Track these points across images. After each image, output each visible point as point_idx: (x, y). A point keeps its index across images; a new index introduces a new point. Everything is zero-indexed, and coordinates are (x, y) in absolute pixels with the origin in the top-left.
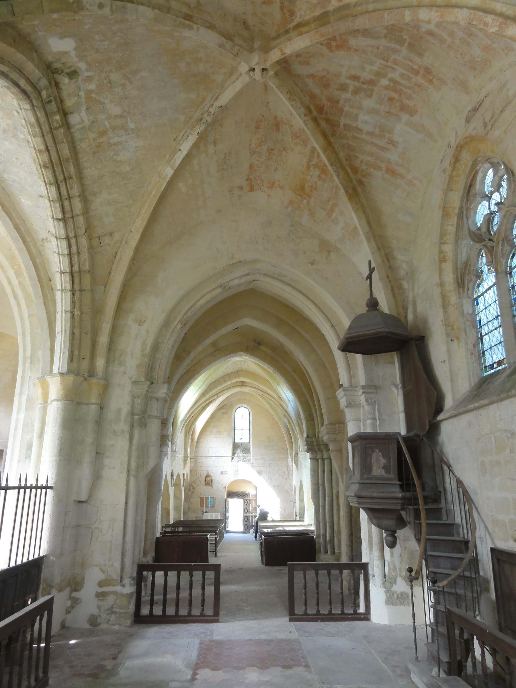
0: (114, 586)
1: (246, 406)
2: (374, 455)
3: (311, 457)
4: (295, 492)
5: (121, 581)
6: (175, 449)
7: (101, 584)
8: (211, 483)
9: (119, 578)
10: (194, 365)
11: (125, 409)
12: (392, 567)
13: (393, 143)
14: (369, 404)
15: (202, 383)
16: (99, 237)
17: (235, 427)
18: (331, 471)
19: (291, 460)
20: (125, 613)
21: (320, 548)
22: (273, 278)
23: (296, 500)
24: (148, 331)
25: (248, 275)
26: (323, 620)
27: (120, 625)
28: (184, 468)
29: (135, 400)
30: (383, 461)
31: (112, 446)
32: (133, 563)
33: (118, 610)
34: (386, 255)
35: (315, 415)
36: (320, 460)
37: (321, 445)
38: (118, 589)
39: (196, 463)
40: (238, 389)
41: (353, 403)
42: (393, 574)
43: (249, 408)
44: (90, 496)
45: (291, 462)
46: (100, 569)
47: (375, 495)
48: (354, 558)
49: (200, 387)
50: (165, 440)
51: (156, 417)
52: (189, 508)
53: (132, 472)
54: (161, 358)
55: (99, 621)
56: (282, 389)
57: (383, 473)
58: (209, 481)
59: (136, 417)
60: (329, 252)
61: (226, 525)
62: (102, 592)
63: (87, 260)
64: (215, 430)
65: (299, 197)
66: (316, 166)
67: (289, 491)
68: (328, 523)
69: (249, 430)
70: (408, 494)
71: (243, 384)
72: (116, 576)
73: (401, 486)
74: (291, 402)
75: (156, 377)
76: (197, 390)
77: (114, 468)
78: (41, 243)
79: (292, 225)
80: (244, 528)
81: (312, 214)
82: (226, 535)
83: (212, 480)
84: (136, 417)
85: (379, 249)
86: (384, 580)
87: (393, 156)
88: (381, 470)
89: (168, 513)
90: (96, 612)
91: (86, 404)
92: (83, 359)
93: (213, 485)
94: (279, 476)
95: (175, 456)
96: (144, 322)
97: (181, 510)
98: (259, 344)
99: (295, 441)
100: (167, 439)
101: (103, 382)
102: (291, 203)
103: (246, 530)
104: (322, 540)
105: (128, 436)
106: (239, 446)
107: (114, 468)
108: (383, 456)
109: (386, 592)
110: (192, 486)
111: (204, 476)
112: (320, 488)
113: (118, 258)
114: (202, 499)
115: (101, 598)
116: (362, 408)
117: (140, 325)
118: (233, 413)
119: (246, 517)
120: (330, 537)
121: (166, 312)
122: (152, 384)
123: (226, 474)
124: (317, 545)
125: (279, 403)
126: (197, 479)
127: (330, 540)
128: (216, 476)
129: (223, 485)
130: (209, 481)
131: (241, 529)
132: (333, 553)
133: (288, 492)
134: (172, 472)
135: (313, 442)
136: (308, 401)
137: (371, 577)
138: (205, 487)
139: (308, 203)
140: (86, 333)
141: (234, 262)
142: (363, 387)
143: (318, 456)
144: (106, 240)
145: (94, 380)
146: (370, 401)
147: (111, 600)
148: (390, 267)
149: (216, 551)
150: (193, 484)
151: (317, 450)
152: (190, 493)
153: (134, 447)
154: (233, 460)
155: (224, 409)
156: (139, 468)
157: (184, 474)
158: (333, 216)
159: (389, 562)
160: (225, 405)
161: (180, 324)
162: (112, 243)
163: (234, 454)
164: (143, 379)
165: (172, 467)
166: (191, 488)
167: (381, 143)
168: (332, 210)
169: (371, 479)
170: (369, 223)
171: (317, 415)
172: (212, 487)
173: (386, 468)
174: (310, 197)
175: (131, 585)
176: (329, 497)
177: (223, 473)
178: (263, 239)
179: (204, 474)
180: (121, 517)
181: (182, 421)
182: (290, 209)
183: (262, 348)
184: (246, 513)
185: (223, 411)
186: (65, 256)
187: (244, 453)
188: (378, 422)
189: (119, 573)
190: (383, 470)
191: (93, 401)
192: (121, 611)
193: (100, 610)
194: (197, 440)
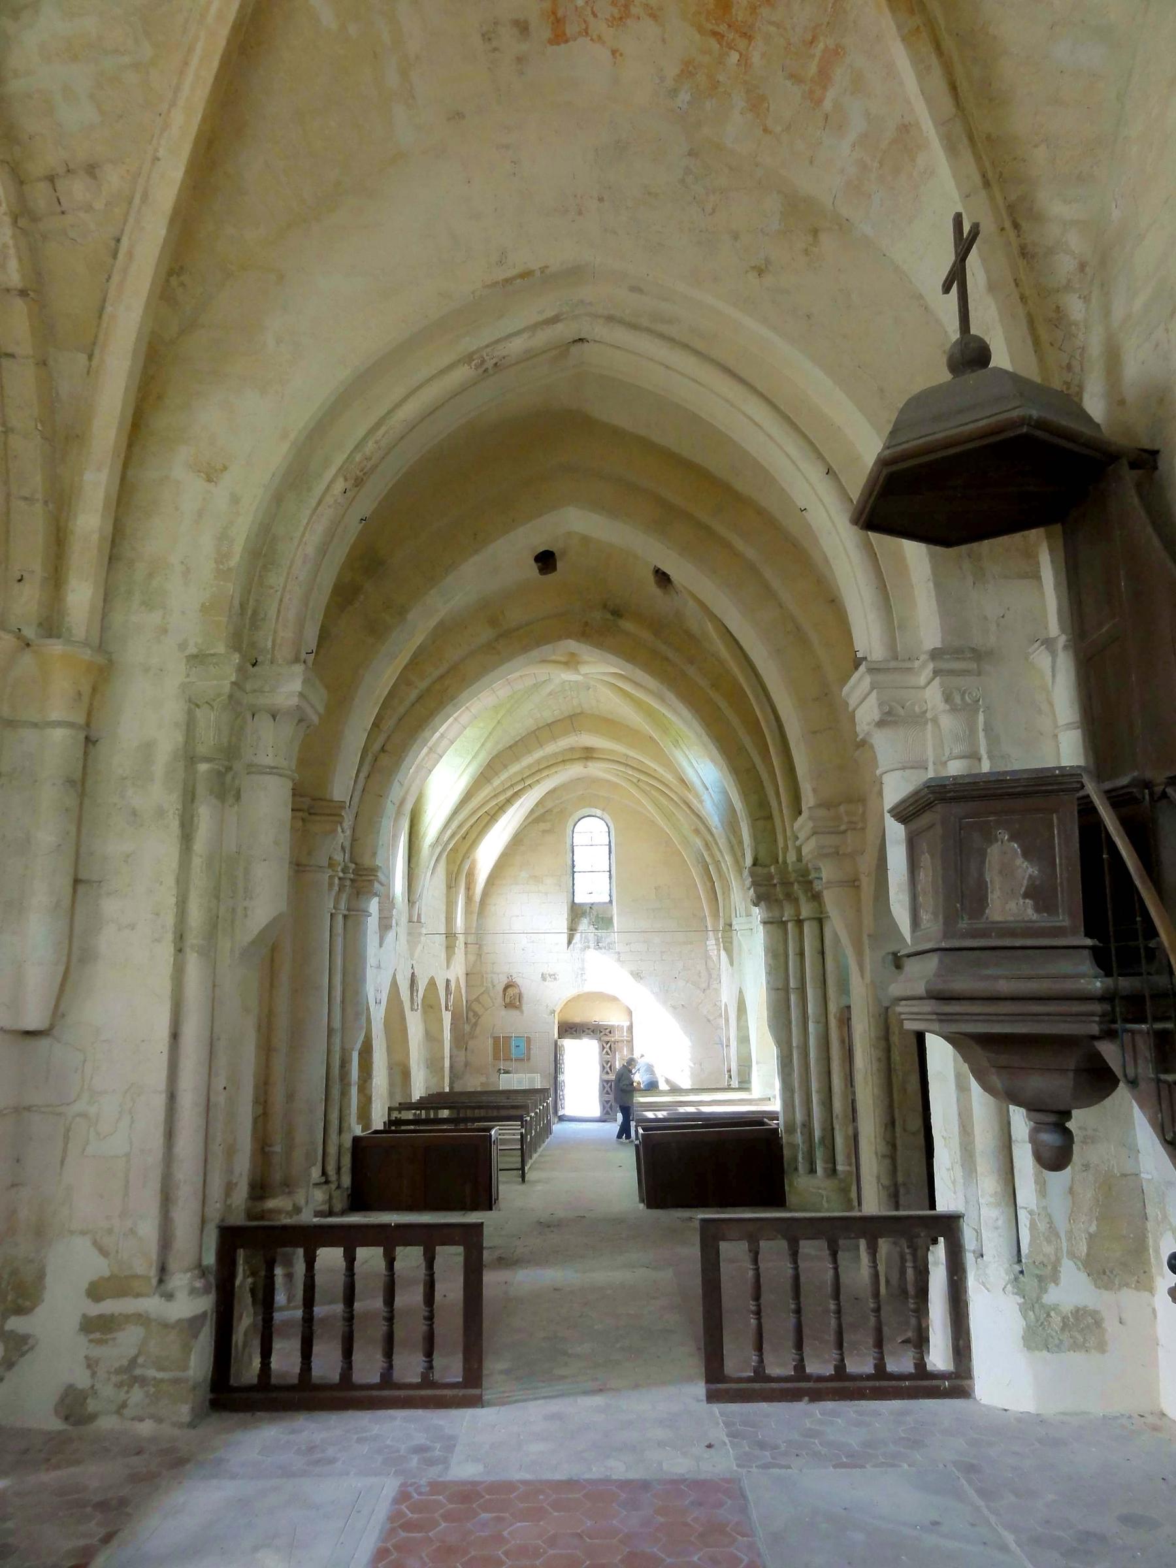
0: (138, 1295)
1: (599, 812)
2: (994, 853)
3: (766, 916)
4: (727, 1020)
5: (161, 1281)
6: (419, 915)
7: (95, 1292)
9: (153, 1273)
10: (442, 677)
11: (168, 743)
12: (1042, 1226)
14: (954, 709)
15: (479, 745)
16: (51, 179)
17: (573, 866)
18: (822, 953)
20: (176, 1381)
21: (795, 1159)
22: (634, 327)
23: (728, 1039)
24: (235, 500)
25: (555, 320)
26: (816, 1396)
27: (159, 1420)
28: (448, 967)
29: (198, 713)
30: (1026, 870)
31: (127, 857)
32: (203, 1222)
33: (152, 1373)
34: (1011, 208)
35: (774, 803)
36: (790, 925)
37: (792, 884)
38: (152, 1305)
39: (479, 955)
40: (575, 770)
41: (902, 712)
42: (1049, 1249)
43: (606, 817)
44: (58, 1013)
45: (715, 947)
46: (95, 1243)
47: (1004, 987)
48: (902, 1191)
49: (474, 757)
50: (369, 881)
51: (273, 770)
52: (467, 1064)
53: (194, 939)
54: (282, 585)
55: (92, 1406)
56: (687, 756)
57: (1030, 911)
58: (512, 997)
59: (203, 767)
60: (815, 232)
61: (559, 1103)
62: (100, 1316)
63: (12, 251)
64: (524, 875)
65: (713, 44)
67: (711, 1018)
68: (817, 1092)
69: (610, 871)
70: (1125, 984)
71: (588, 755)
72: (144, 1266)
73: (1101, 959)
74: (710, 790)
75: (269, 644)
76: (468, 764)
77: (132, 927)
79: (692, 153)
81: (757, 104)
82: (557, 1128)
83: (520, 995)
84: (203, 767)
85: (987, 184)
86: (1017, 1268)
88: (1021, 901)
89: (406, 1075)
90: (82, 1379)
91: (35, 725)
92: (20, 581)
93: (525, 1007)
95: (420, 934)
96: (222, 471)
97: (443, 1068)
98: (617, 613)
99: (724, 893)
100: (372, 878)
101: (87, 655)
102: (688, 70)
103: (607, 1113)
104: (799, 1138)
105: (175, 825)
107: (133, 929)
108: (1026, 854)
109: (1024, 1310)
111: (500, 988)
112: (793, 998)
113: (121, 256)
114: (496, 1040)
115: (98, 1335)
116: (929, 726)
117: (209, 480)
118: (569, 831)
120: (823, 1130)
121: (292, 436)
122: (254, 665)
123: (555, 979)
124: (786, 1152)
125: (681, 798)
126: (482, 993)
127: (823, 1139)
128: (529, 984)
129: (547, 1006)
130: (514, 999)
131: (596, 1112)
132: (833, 1172)
133: (709, 1021)
134: (413, 973)
135: (771, 877)
136: (754, 767)
137: (969, 1259)
138: (504, 1012)
139: (745, 61)
140: (26, 499)
141: (510, 273)
142: (935, 654)
143: (786, 914)
144: (77, 189)
145: (56, 648)
146: (958, 700)
147: (128, 1340)
148: (1024, 252)
149: (523, 1169)
150: (477, 1007)
151: (781, 897)
152: (467, 1028)
153: (197, 862)
154: (572, 945)
155: (544, 822)
156: (213, 926)
157: (448, 981)
158: (828, 105)
159: (1031, 1213)
161: (341, 479)
162: (99, 205)
163: (572, 930)
164: (221, 648)
165: (414, 962)
166: (471, 1014)
168: (824, 77)
169: (984, 934)
170: (953, 88)
171: (780, 803)
172: (522, 1012)
173: (1039, 894)
174: (748, 36)
175: (193, 1291)
176: (818, 1023)
177: (548, 979)
178: (601, 200)
179: (504, 981)
180: (157, 1077)
181: (433, 846)
182: (684, 97)
183: (628, 625)
184: (607, 1073)
185: (543, 826)
189: (154, 1256)
190: (1027, 901)
191: (54, 716)
192: (160, 1375)
193: (94, 1374)
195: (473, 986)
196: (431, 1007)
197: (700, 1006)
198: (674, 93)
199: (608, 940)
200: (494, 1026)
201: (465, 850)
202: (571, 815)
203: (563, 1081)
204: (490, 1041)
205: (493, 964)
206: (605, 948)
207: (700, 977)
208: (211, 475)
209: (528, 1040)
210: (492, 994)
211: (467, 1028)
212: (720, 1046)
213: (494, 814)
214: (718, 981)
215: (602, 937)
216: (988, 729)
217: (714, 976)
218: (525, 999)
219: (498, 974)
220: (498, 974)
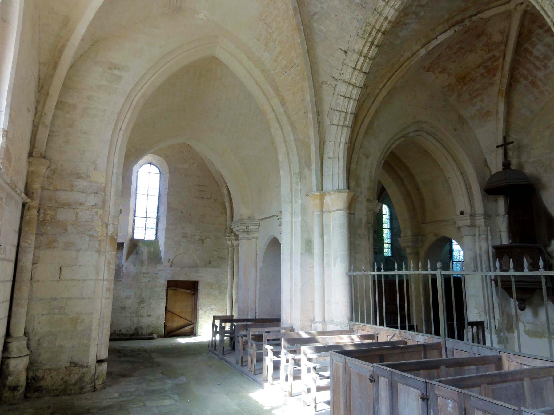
13: (546, 66)
22: (430, 135)
24: (372, 164)
25: (417, 131)
65: (457, 83)
66: (486, 67)
78: (320, 84)
81: (459, 96)
86: (496, 330)
87: (540, 74)
102: (449, 85)
105: (367, 238)
109: (498, 337)
158: (474, 101)
159: (498, 320)
167: (538, 64)
168: (475, 97)
182: (446, 89)
186: (356, 101)
188: (489, 237)
198: (444, 88)
208: (367, 157)
216: (490, 230)
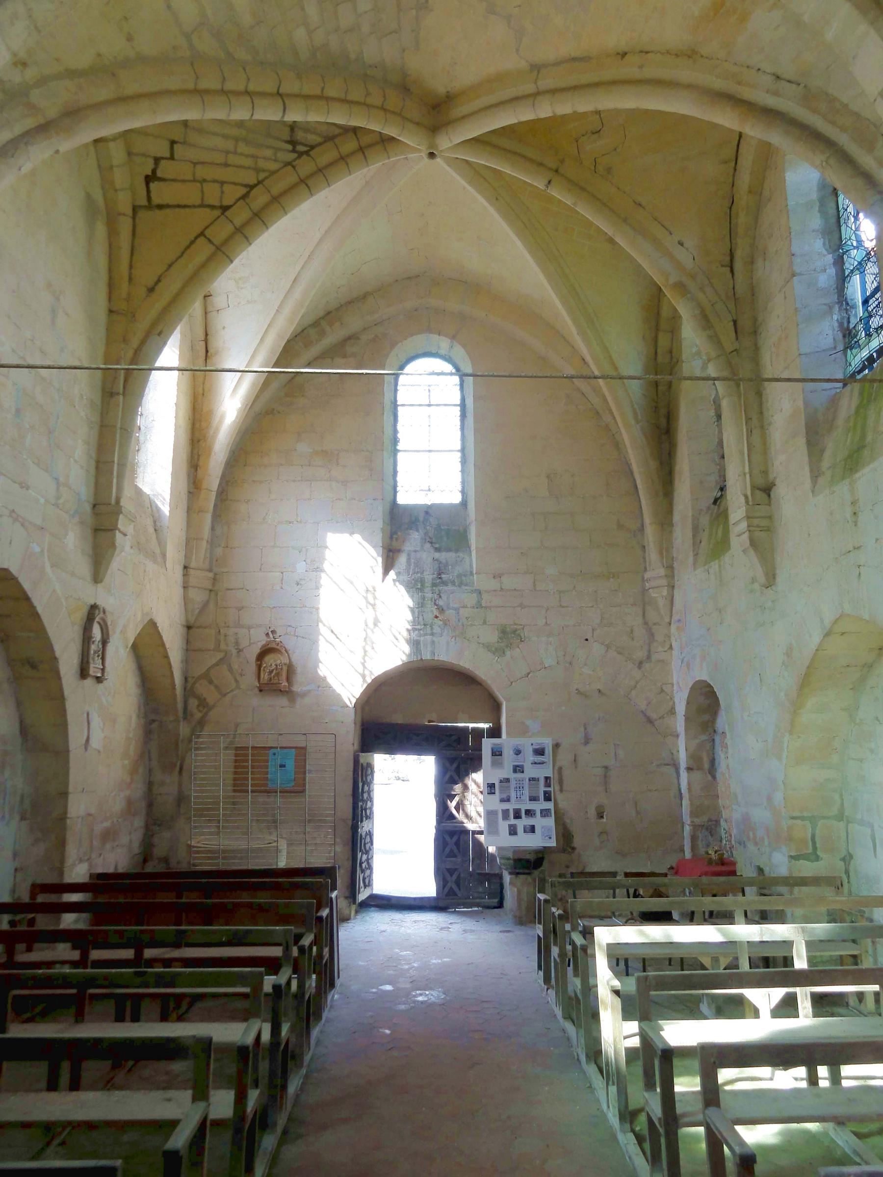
1: (444, 343)
8: (285, 683)
19: (662, 572)
45: (664, 582)
61: (360, 876)
64: (303, 448)
67: (654, 716)
80: (444, 887)
83: (291, 670)
93: (296, 688)
94: (608, 647)
103: (451, 893)
106: (417, 520)
110: (198, 697)
111: (256, 650)
114: (240, 753)
119: (452, 833)
126: (217, 664)
130: (278, 675)
131: (428, 888)
133: (650, 721)
138: (256, 701)
150: (203, 689)
160: (349, 338)
179: (259, 640)
187: (437, 550)
194: (223, 494)
195: (200, 650)
196: (34, 666)
197: (633, 693)
199: (458, 570)
200: (237, 726)
201: (153, 313)
202: (393, 345)
203: (370, 834)
204: (226, 759)
205: (240, 609)
206: (453, 583)
207: (633, 639)
209: (301, 752)
210: (235, 667)
211: (184, 729)
212: (670, 770)
213: (226, 242)
214: (667, 647)
215: (447, 564)
217: (659, 637)
218: (299, 678)
219: (249, 628)
220: (249, 628)
